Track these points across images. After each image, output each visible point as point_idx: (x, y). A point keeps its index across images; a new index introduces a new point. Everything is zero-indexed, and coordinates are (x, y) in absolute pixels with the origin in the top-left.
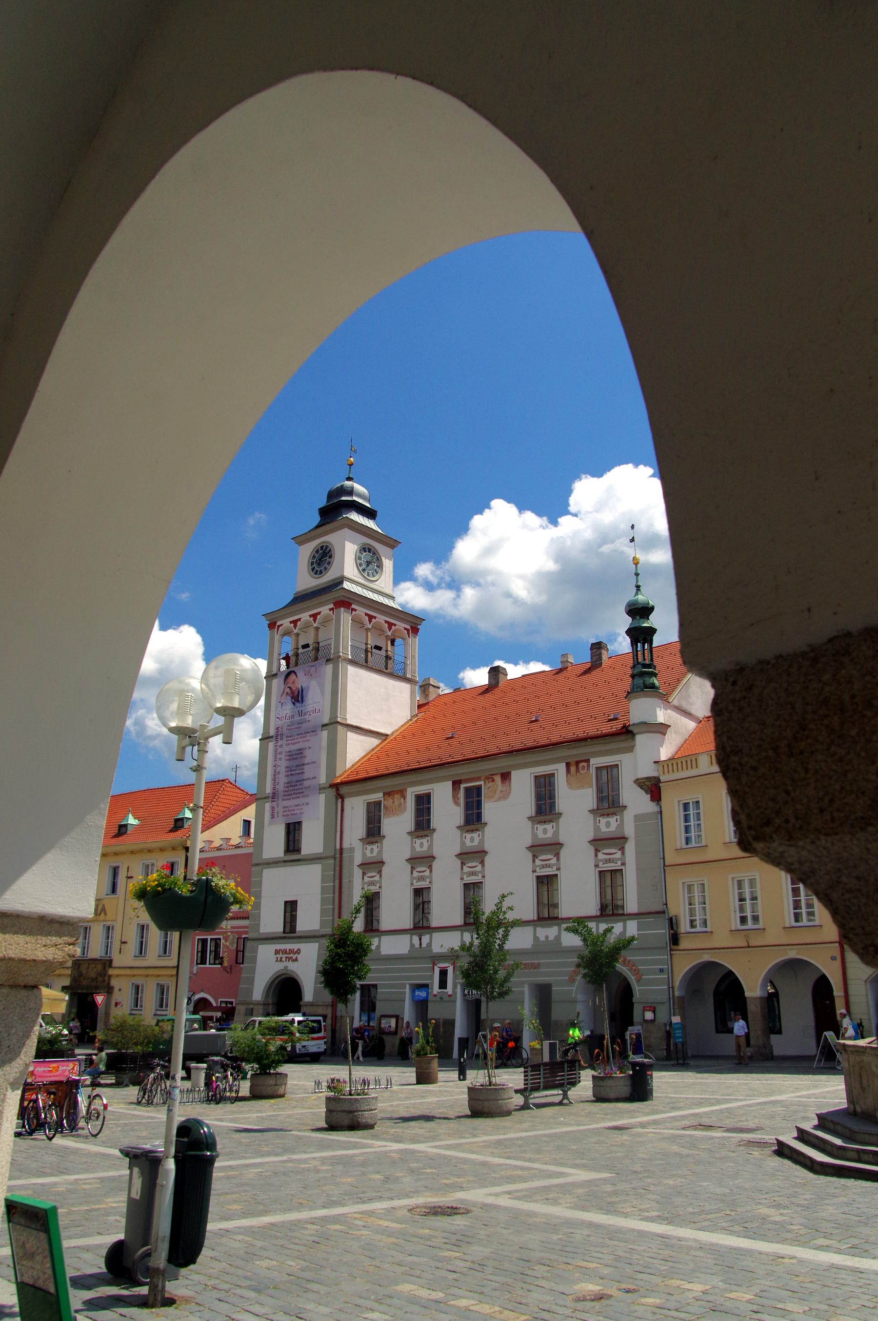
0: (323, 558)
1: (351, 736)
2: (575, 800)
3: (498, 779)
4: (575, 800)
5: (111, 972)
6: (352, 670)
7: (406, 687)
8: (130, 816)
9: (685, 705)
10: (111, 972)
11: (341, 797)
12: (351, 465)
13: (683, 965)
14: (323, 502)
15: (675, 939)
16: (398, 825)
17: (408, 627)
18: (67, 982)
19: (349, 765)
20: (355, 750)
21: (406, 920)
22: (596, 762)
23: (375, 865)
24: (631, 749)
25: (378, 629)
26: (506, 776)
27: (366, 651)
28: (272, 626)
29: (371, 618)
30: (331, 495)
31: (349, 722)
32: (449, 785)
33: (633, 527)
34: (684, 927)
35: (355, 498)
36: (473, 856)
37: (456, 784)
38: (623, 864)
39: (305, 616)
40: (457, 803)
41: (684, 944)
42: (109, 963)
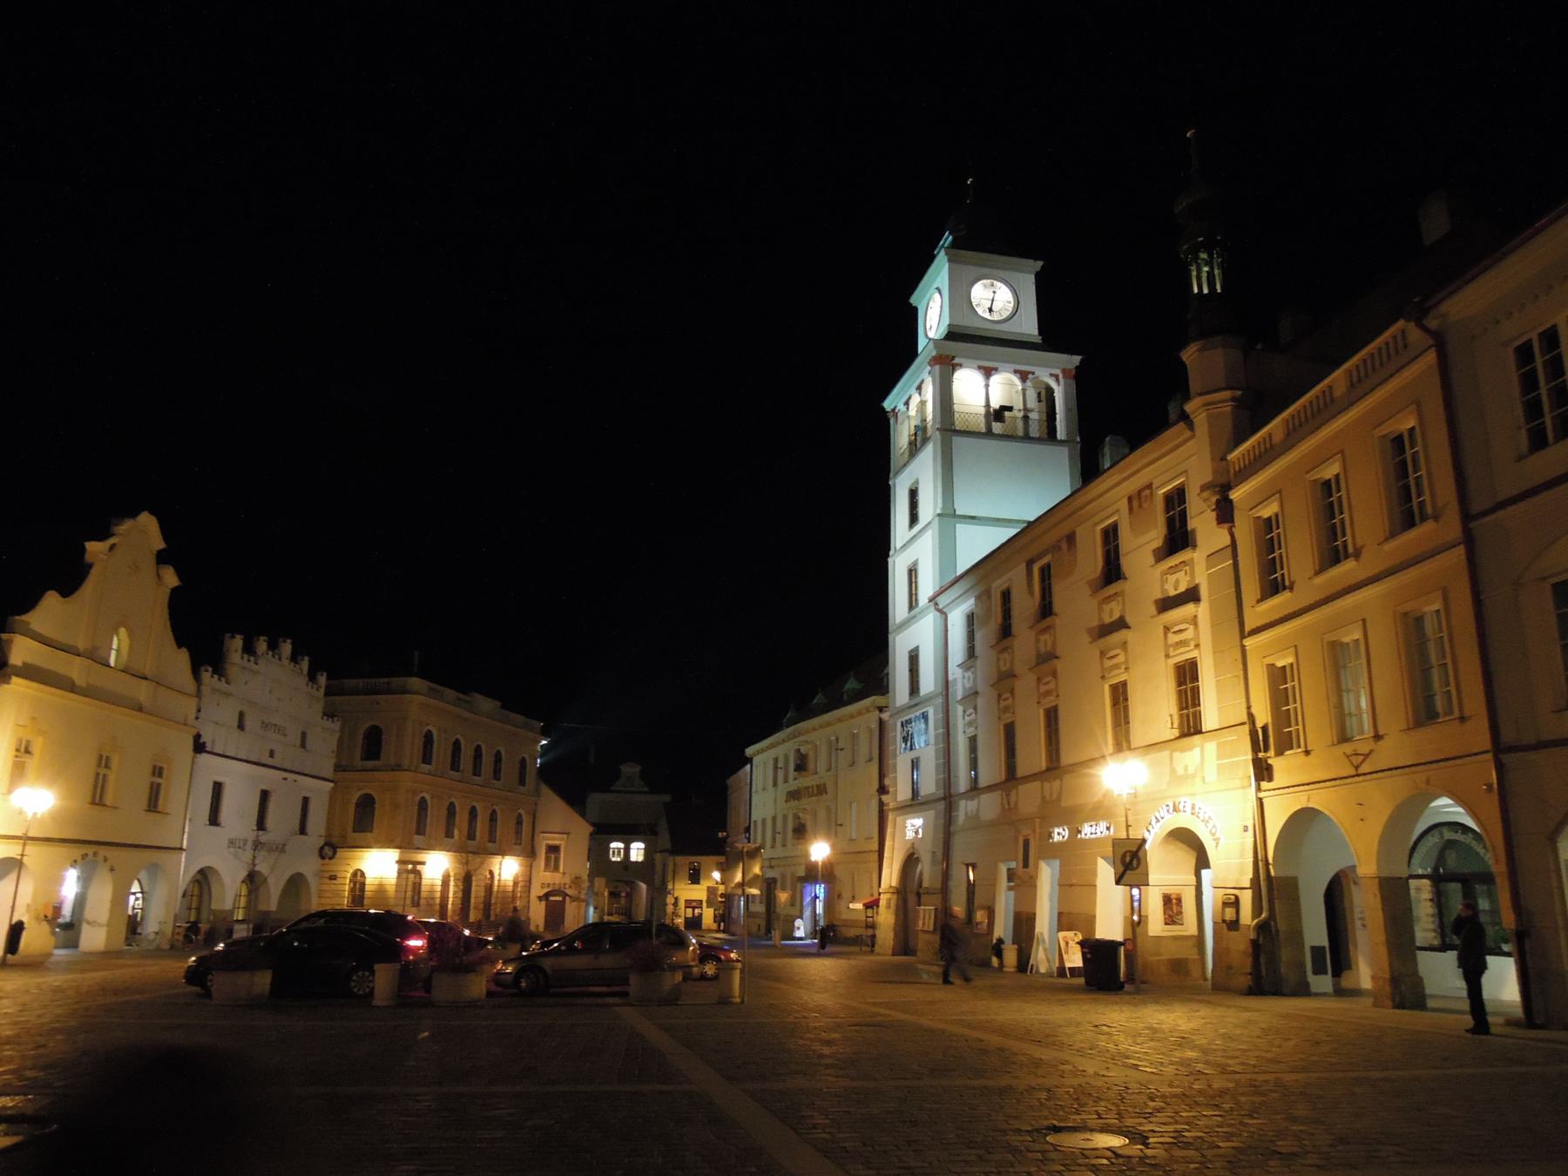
1: (963, 530)
3: (1064, 545)
11: (943, 614)
17: (1058, 372)
27: (988, 414)
32: (1022, 568)
37: (1030, 564)
38: (1197, 646)
40: (1031, 593)
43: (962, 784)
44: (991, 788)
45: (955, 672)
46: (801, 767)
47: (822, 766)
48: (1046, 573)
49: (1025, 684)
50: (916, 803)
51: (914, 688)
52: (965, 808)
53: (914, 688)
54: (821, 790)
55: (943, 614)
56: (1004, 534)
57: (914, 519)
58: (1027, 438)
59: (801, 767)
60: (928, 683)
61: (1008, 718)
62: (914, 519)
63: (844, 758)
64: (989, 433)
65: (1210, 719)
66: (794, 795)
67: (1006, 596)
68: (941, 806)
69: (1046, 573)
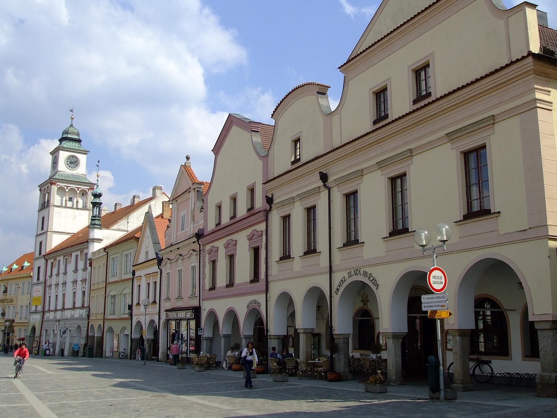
0: (55, 163)
1: (55, 236)
2: (81, 265)
5: (14, 324)
6: (56, 209)
8: (26, 262)
9: (122, 228)
10: (14, 324)
11: (47, 260)
12: (72, 119)
15: (88, 316)
16: (55, 271)
18: (3, 328)
19: (53, 247)
20: (55, 241)
22: (85, 251)
24: (87, 248)
25: (72, 190)
26: (71, 254)
28: (40, 190)
29: (67, 187)
31: (54, 230)
33: (99, 162)
35: (69, 136)
36: (64, 284)
37: (64, 256)
39: (46, 187)
42: (13, 321)
43: (47, 309)
44: (52, 311)
45: (48, 278)
46: (5, 292)
47: (13, 293)
49: (60, 286)
50: (36, 312)
51: (38, 279)
52: (47, 315)
53: (38, 279)
54: (12, 301)
55: (47, 260)
56: (66, 237)
57: (42, 229)
58: (78, 209)
59: (5, 292)
60: (42, 279)
61: (57, 294)
62: (42, 229)
63: (20, 290)
64: (66, 207)
65: (86, 305)
66: (3, 301)
68: (42, 313)
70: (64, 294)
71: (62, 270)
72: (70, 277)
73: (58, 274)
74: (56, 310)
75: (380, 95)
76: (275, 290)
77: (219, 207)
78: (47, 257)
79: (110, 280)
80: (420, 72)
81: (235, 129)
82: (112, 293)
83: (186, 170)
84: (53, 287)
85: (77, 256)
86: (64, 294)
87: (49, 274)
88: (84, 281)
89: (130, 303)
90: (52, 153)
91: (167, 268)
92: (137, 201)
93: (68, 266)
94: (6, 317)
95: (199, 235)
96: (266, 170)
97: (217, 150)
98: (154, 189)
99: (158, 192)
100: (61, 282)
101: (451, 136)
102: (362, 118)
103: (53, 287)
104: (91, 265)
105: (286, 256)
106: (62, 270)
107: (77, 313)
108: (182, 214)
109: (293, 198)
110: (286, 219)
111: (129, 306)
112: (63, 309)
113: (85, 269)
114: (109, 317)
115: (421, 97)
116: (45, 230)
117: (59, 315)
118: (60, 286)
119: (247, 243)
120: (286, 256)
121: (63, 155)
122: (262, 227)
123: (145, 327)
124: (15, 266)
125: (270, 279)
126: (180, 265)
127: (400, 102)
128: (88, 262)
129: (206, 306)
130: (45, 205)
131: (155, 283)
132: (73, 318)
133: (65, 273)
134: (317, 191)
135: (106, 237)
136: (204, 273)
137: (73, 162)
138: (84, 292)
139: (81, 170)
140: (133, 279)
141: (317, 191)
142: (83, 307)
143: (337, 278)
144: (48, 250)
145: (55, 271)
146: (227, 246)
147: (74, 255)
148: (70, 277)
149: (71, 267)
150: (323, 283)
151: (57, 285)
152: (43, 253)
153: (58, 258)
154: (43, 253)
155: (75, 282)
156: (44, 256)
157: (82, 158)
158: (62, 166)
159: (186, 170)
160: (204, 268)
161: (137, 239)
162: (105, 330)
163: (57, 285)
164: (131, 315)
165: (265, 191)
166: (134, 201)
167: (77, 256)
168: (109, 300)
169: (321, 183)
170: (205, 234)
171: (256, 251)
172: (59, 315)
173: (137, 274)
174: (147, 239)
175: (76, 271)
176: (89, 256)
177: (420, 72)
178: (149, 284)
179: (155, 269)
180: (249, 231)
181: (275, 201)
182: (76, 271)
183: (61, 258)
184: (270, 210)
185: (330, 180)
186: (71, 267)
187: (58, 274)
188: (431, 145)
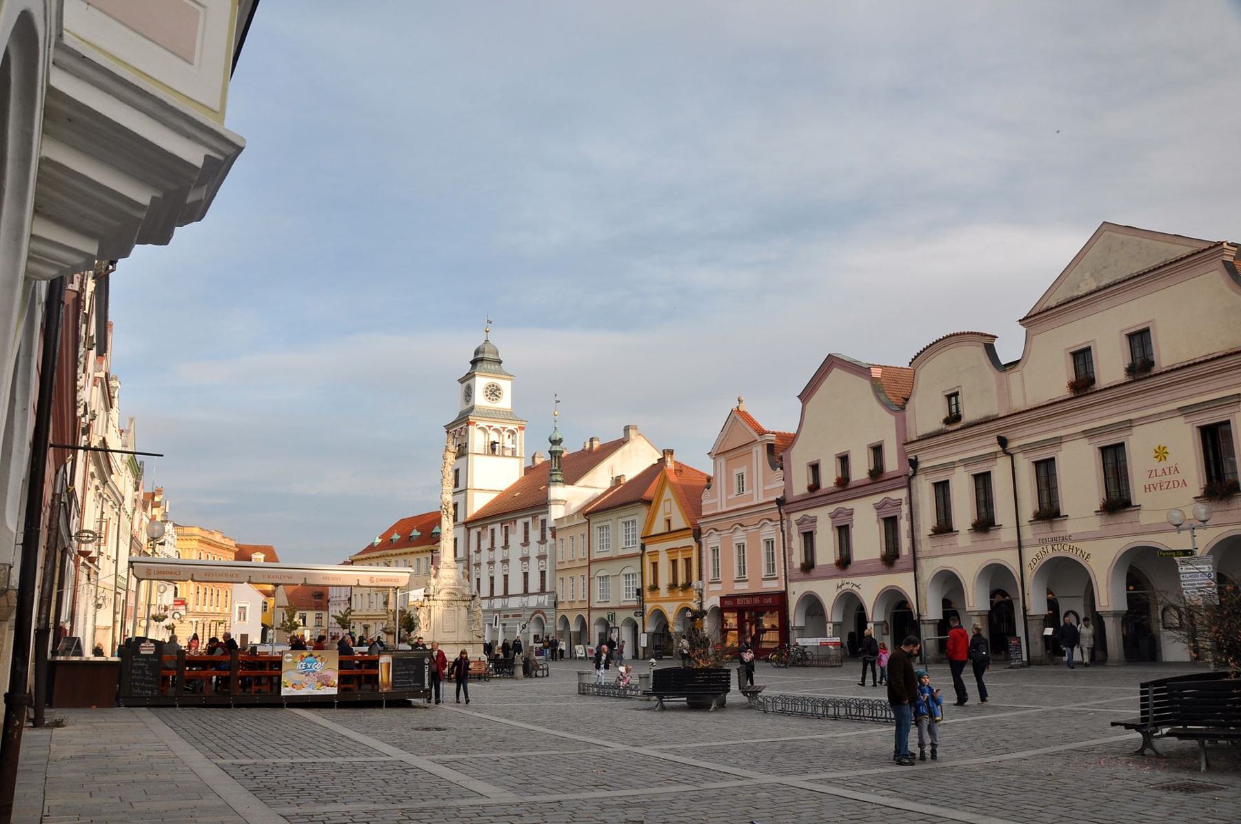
0: (469, 393)
1: (477, 495)
2: (535, 535)
4: (535, 535)
6: (476, 457)
7: (516, 461)
9: (589, 484)
11: (469, 529)
13: (559, 616)
14: (472, 358)
16: (486, 544)
20: (478, 503)
21: (488, 594)
22: (541, 517)
23: (478, 565)
30: (477, 352)
34: (560, 599)
35: (486, 356)
36: (505, 561)
39: (458, 428)
41: (560, 607)
48: (506, 528)
49: (498, 564)
55: (469, 529)
56: (493, 496)
57: (456, 485)
65: (548, 589)
67: (493, 530)
69: (506, 528)
70: (506, 577)
71: (499, 540)
72: (516, 551)
73: (492, 548)
74: (492, 596)
75: (1082, 357)
76: (928, 569)
77: (815, 468)
78: (469, 524)
79: (595, 556)
80: (1140, 339)
81: (836, 373)
82: (600, 574)
83: (739, 417)
84: (484, 566)
85: (526, 525)
86: (506, 577)
87: (474, 547)
88: (541, 557)
89: (639, 586)
90: (462, 381)
91: (710, 541)
92: (596, 445)
93: (511, 537)
94: (391, 607)
95: (780, 502)
96: (901, 427)
97: (805, 396)
98: (627, 429)
99: (632, 433)
100: (498, 558)
101: (1184, 411)
102: (1054, 380)
103: (484, 566)
104: (554, 536)
105: (944, 527)
106: (499, 540)
107: (533, 602)
108: (736, 471)
109: (953, 463)
110: (942, 489)
111: (638, 591)
112: (506, 594)
113: (543, 540)
114: (597, 606)
115: (1141, 365)
116: (461, 487)
117: (498, 604)
118: (498, 564)
119: (875, 512)
120: (944, 527)
121: (481, 383)
122: (902, 494)
123: (671, 617)
124: (396, 537)
125: (919, 555)
126: (740, 536)
127: (1111, 366)
128: (548, 534)
129: (796, 591)
130: (462, 452)
131: (688, 561)
132: (525, 608)
133: (506, 546)
134: (992, 457)
135: (567, 498)
136: (790, 548)
137: (494, 392)
138: (543, 574)
139: (505, 403)
140: (642, 556)
141: (992, 457)
142: (543, 590)
143: (1030, 554)
144: (469, 515)
145: (486, 544)
146: (833, 516)
147: (520, 523)
148: (516, 551)
149: (516, 537)
150: (1009, 559)
151: (491, 563)
152: (461, 519)
153: (490, 527)
154: (461, 519)
155: (525, 559)
156: (465, 523)
157: (505, 385)
158: (480, 399)
159: (739, 417)
160: (790, 540)
161: (648, 502)
162: (593, 621)
163: (491, 563)
164: (642, 601)
165: (902, 454)
166: (591, 445)
167: (526, 525)
168: (596, 584)
169: (998, 448)
170: (789, 500)
171: (890, 524)
172: (498, 604)
173: (649, 548)
174: (668, 503)
175: (526, 542)
176: (551, 523)
177: (1140, 339)
178: (674, 562)
179: (690, 541)
180: (878, 499)
181: (922, 466)
182: (526, 542)
183: (497, 527)
184: (914, 475)
185: (1011, 445)
186: (516, 537)
187: (492, 548)
188: (1158, 417)
